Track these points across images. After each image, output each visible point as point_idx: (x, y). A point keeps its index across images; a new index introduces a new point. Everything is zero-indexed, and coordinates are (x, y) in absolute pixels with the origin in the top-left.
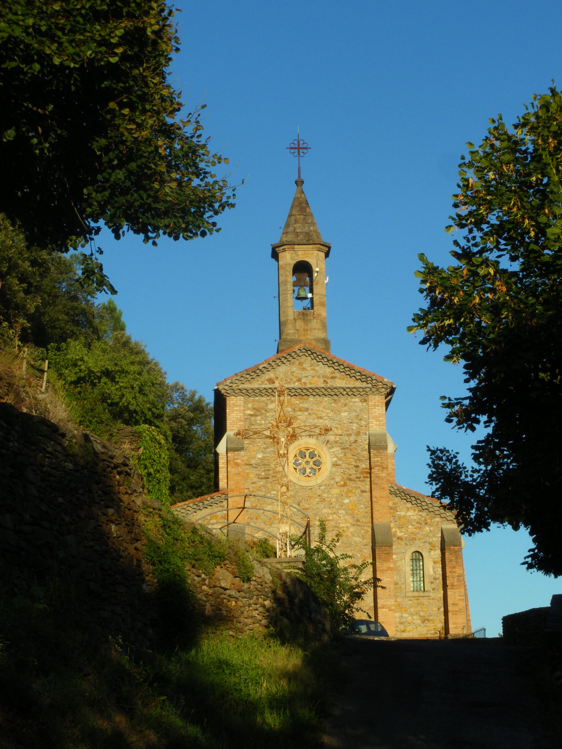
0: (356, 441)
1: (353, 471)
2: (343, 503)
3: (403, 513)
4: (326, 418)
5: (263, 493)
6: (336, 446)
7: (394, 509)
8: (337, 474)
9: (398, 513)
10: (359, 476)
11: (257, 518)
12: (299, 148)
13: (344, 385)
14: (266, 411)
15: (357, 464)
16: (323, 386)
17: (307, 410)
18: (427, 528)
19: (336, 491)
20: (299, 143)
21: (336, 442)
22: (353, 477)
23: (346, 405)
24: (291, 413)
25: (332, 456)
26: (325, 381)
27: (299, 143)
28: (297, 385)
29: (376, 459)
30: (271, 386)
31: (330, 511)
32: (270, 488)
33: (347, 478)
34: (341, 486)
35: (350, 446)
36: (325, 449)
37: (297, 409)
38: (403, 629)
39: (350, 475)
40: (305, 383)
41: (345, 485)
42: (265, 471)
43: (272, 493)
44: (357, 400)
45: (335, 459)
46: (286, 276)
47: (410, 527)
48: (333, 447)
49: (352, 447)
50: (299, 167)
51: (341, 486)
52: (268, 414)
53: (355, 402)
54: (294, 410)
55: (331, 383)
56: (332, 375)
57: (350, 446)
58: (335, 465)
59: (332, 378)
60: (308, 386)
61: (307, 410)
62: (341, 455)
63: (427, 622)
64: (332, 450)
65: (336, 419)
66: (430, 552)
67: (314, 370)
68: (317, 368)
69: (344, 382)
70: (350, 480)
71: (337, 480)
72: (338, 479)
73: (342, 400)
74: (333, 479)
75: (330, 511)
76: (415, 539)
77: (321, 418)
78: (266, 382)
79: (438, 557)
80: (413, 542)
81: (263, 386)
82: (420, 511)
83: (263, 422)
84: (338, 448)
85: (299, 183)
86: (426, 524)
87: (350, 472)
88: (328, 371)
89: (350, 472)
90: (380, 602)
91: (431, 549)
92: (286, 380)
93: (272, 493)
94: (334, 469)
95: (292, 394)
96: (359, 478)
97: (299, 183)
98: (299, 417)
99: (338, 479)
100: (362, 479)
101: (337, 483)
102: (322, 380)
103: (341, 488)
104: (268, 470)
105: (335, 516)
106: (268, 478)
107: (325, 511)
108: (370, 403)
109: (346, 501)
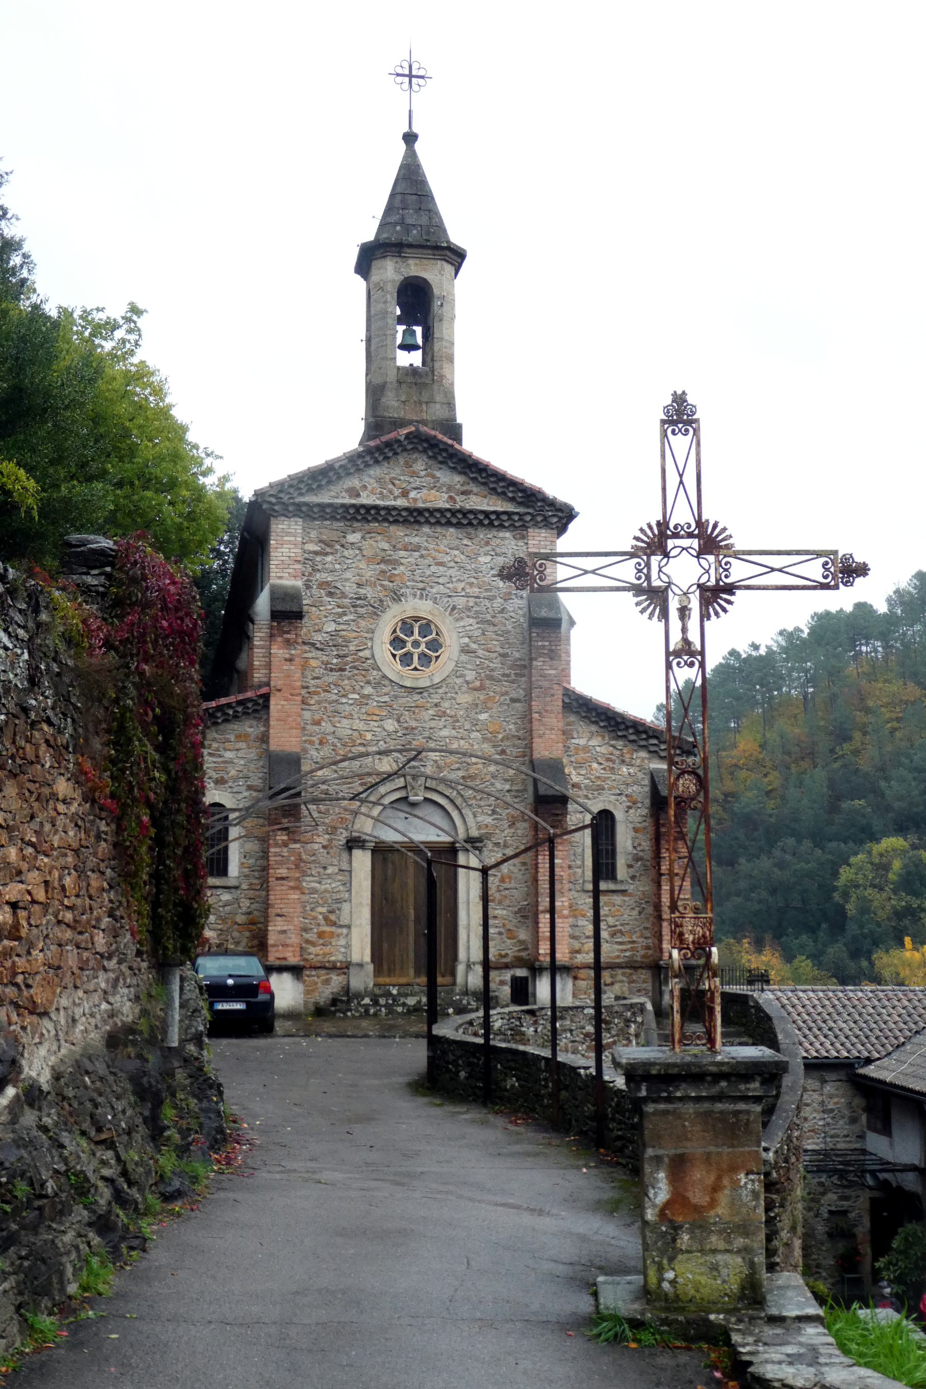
0: (503, 611)
1: (496, 664)
2: (478, 720)
3: (582, 742)
4: (452, 564)
5: (335, 697)
6: (468, 617)
7: (567, 734)
8: (469, 667)
9: (573, 741)
10: (507, 672)
11: (321, 743)
12: (410, 76)
13: (485, 508)
14: (342, 546)
15: (506, 651)
16: (448, 506)
17: (417, 548)
18: (625, 770)
19: (465, 698)
20: (410, 67)
21: (469, 609)
22: (496, 674)
23: (487, 544)
24: (388, 552)
25: (461, 634)
26: (451, 497)
27: (410, 67)
28: (401, 502)
29: (540, 644)
30: (353, 501)
31: (454, 733)
32: (347, 688)
33: (487, 676)
34: (475, 689)
35: (493, 617)
36: (449, 619)
37: (399, 546)
38: (577, 948)
39: (492, 670)
40: (415, 500)
41: (481, 688)
42: (339, 656)
43: (351, 696)
44: (508, 535)
45: (466, 640)
46: (385, 302)
47: (595, 765)
48: (462, 618)
49: (495, 621)
50: (410, 111)
51: (475, 689)
52: (346, 553)
53: (503, 539)
54: (394, 547)
55: (462, 502)
56: (465, 488)
57: (493, 617)
58: (465, 650)
59: (463, 493)
60: (420, 505)
61: (417, 548)
62: (476, 633)
63: (619, 935)
64: (462, 624)
65: (469, 567)
66: (627, 812)
67: (433, 477)
68: (438, 474)
69: (486, 501)
70: (491, 678)
71: (467, 678)
72: (470, 675)
73: (482, 534)
74: (462, 676)
75: (454, 733)
76: (603, 789)
77: (441, 564)
78: (344, 494)
79: (560, 848)
80: (599, 794)
81: (340, 501)
82: (611, 739)
83: (337, 566)
84: (471, 621)
85: (410, 138)
86: (623, 761)
87: (491, 665)
88: (457, 479)
89: (491, 665)
90: (491, 912)
91: (630, 807)
92: (381, 493)
93: (351, 696)
94: (464, 658)
95: (391, 519)
96: (508, 676)
97: (410, 138)
98: (402, 561)
99: (470, 675)
100: (513, 677)
101: (468, 683)
102: (446, 496)
103: (475, 692)
104: (345, 656)
105: (462, 742)
106: (344, 670)
107: (445, 733)
108: (530, 542)
109: (483, 717)
